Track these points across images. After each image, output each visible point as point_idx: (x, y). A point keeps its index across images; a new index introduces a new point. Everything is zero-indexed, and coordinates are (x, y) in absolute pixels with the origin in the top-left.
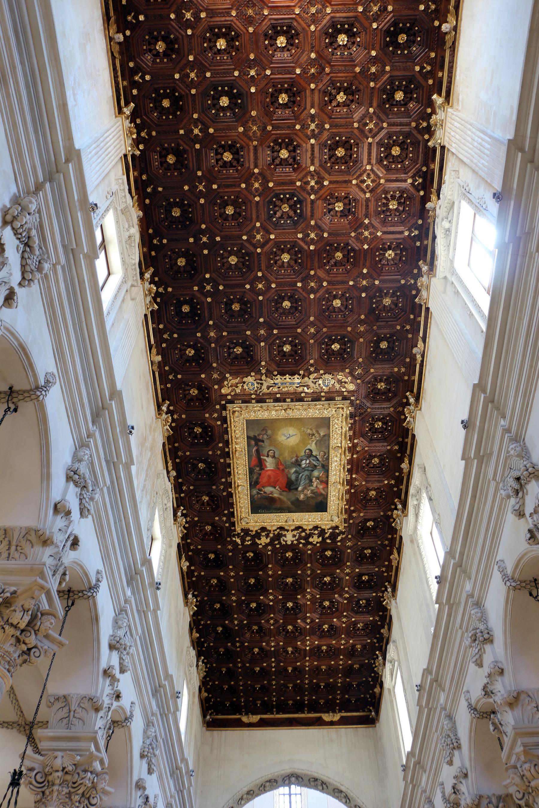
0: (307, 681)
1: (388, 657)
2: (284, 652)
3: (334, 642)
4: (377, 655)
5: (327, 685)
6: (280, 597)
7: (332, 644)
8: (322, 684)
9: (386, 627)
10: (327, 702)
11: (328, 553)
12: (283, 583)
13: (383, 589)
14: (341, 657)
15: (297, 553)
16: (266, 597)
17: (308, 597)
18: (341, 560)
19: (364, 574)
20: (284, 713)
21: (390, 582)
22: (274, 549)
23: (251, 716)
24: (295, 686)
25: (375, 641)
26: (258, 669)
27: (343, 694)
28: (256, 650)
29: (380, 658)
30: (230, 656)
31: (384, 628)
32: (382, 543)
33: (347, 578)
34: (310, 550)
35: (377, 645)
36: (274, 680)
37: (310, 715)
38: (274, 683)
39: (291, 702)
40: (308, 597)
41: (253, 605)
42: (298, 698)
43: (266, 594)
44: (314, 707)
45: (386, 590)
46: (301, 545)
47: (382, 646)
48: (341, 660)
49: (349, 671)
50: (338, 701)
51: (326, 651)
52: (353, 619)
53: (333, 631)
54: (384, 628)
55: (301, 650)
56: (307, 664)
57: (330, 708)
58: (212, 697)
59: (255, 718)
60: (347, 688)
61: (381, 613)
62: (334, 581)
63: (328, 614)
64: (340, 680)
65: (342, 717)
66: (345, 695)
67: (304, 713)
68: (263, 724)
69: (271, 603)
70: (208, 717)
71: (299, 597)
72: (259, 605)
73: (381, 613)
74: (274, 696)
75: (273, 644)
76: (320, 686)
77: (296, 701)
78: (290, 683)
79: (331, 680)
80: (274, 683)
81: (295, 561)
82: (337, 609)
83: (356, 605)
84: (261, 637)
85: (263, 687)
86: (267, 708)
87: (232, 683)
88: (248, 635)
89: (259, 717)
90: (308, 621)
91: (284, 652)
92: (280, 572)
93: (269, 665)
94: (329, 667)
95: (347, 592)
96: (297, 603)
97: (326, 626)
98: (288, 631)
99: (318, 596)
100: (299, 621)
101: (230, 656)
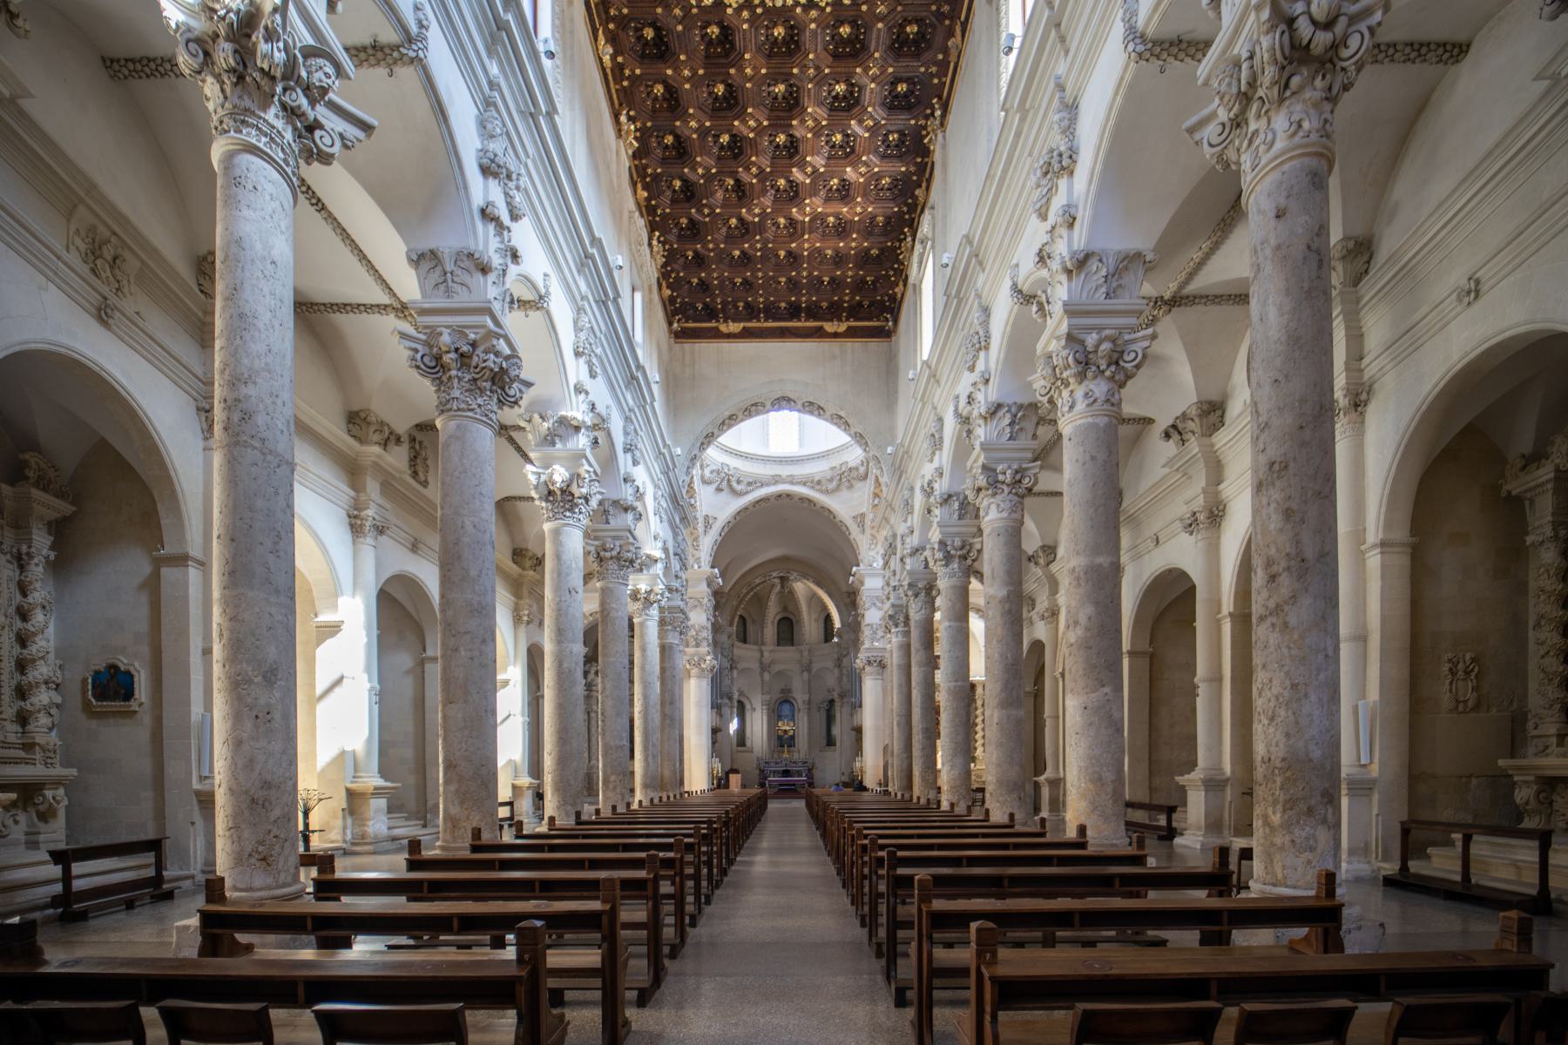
0: (805, 274)
1: (919, 235)
2: (773, 224)
3: (845, 210)
4: (905, 234)
5: (833, 280)
6: (765, 123)
7: (841, 213)
8: (826, 279)
9: (924, 185)
10: (832, 305)
11: (845, 30)
12: (769, 93)
13: (929, 111)
14: (854, 236)
15: (792, 27)
16: (744, 122)
17: (810, 123)
18: (864, 47)
19: (900, 80)
20: (775, 320)
21: (940, 98)
22: (753, 20)
23: (731, 324)
24: (790, 279)
25: (905, 209)
26: (737, 253)
27: (853, 294)
28: (733, 221)
29: (909, 239)
30: (694, 231)
31: (920, 186)
32: (938, 9)
33: (873, 85)
34: (814, 20)
35: (907, 217)
36: (759, 270)
37: (808, 324)
38: (760, 274)
39: (783, 305)
40: (810, 123)
41: (725, 139)
42: (793, 299)
43: (742, 116)
44: (813, 313)
45: (932, 114)
46: (799, 10)
47: (914, 219)
48: (854, 240)
49: (864, 259)
50: (845, 305)
51: (834, 226)
52: (876, 170)
53: (845, 192)
54: (920, 186)
55: (797, 222)
56: (806, 246)
57: (834, 312)
58: (677, 297)
59: (735, 327)
60: (860, 285)
61: (919, 160)
62: (852, 93)
63: (840, 158)
64: (850, 273)
65: (849, 328)
66: (855, 295)
67: (800, 321)
68: (747, 334)
69: (751, 135)
70: (675, 325)
71: (794, 123)
72: (733, 136)
73: (919, 160)
74: (761, 296)
75: (757, 211)
76: (823, 282)
77: (790, 304)
78: (783, 276)
79: (838, 273)
80: (760, 274)
81: (788, 48)
82: (853, 150)
83: (883, 142)
84: (740, 198)
85: (746, 282)
86: (752, 312)
87: (703, 275)
88: (720, 195)
89: (742, 325)
90: (809, 170)
91: (773, 224)
92: (763, 71)
93: (752, 247)
94: (837, 252)
95: (871, 117)
96: (791, 136)
97: (836, 181)
98: (778, 190)
99: (824, 123)
100: (794, 170)
101: (694, 231)
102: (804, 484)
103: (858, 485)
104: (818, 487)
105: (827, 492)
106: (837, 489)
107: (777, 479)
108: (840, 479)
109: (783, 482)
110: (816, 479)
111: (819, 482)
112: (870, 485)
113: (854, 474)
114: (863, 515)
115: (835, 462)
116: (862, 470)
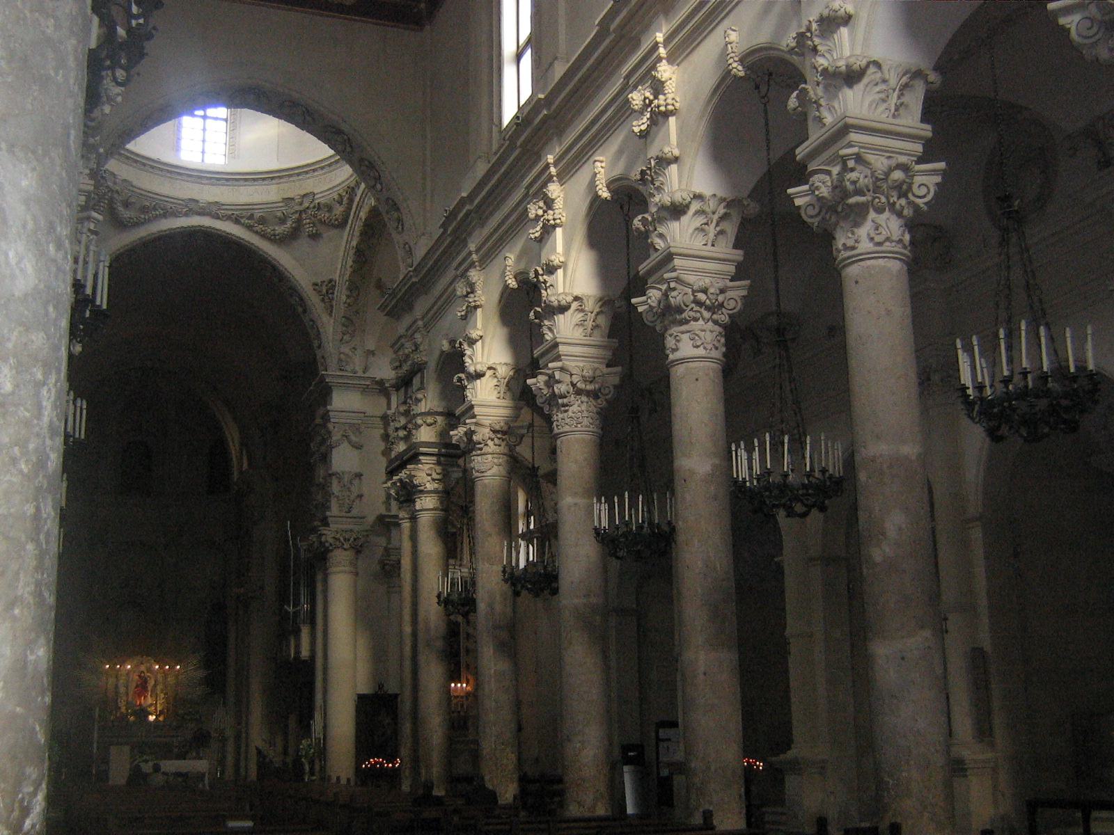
102: (237, 221)
103: (328, 234)
104: (259, 228)
105: (272, 239)
106: (294, 234)
107: (193, 208)
108: (299, 221)
109: (202, 213)
110: (257, 215)
111: (262, 221)
112: (351, 235)
113: (323, 215)
114: (331, 284)
115: (295, 189)
116: (339, 210)
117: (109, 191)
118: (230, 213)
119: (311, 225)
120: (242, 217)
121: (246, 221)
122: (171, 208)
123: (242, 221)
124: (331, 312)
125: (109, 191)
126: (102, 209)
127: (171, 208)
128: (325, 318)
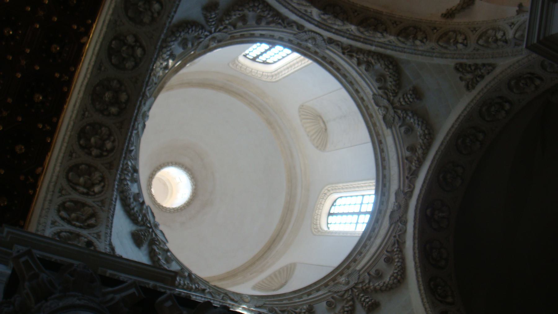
105: (430, 135)
113: (390, 83)
117: (352, 291)
118: (407, 181)
119: (405, 96)
120: (410, 169)
121: (413, 164)
122: (395, 237)
123: (414, 168)
124: (490, 65)
125: (352, 291)
126: (367, 300)
127: (395, 237)
128: (498, 71)
